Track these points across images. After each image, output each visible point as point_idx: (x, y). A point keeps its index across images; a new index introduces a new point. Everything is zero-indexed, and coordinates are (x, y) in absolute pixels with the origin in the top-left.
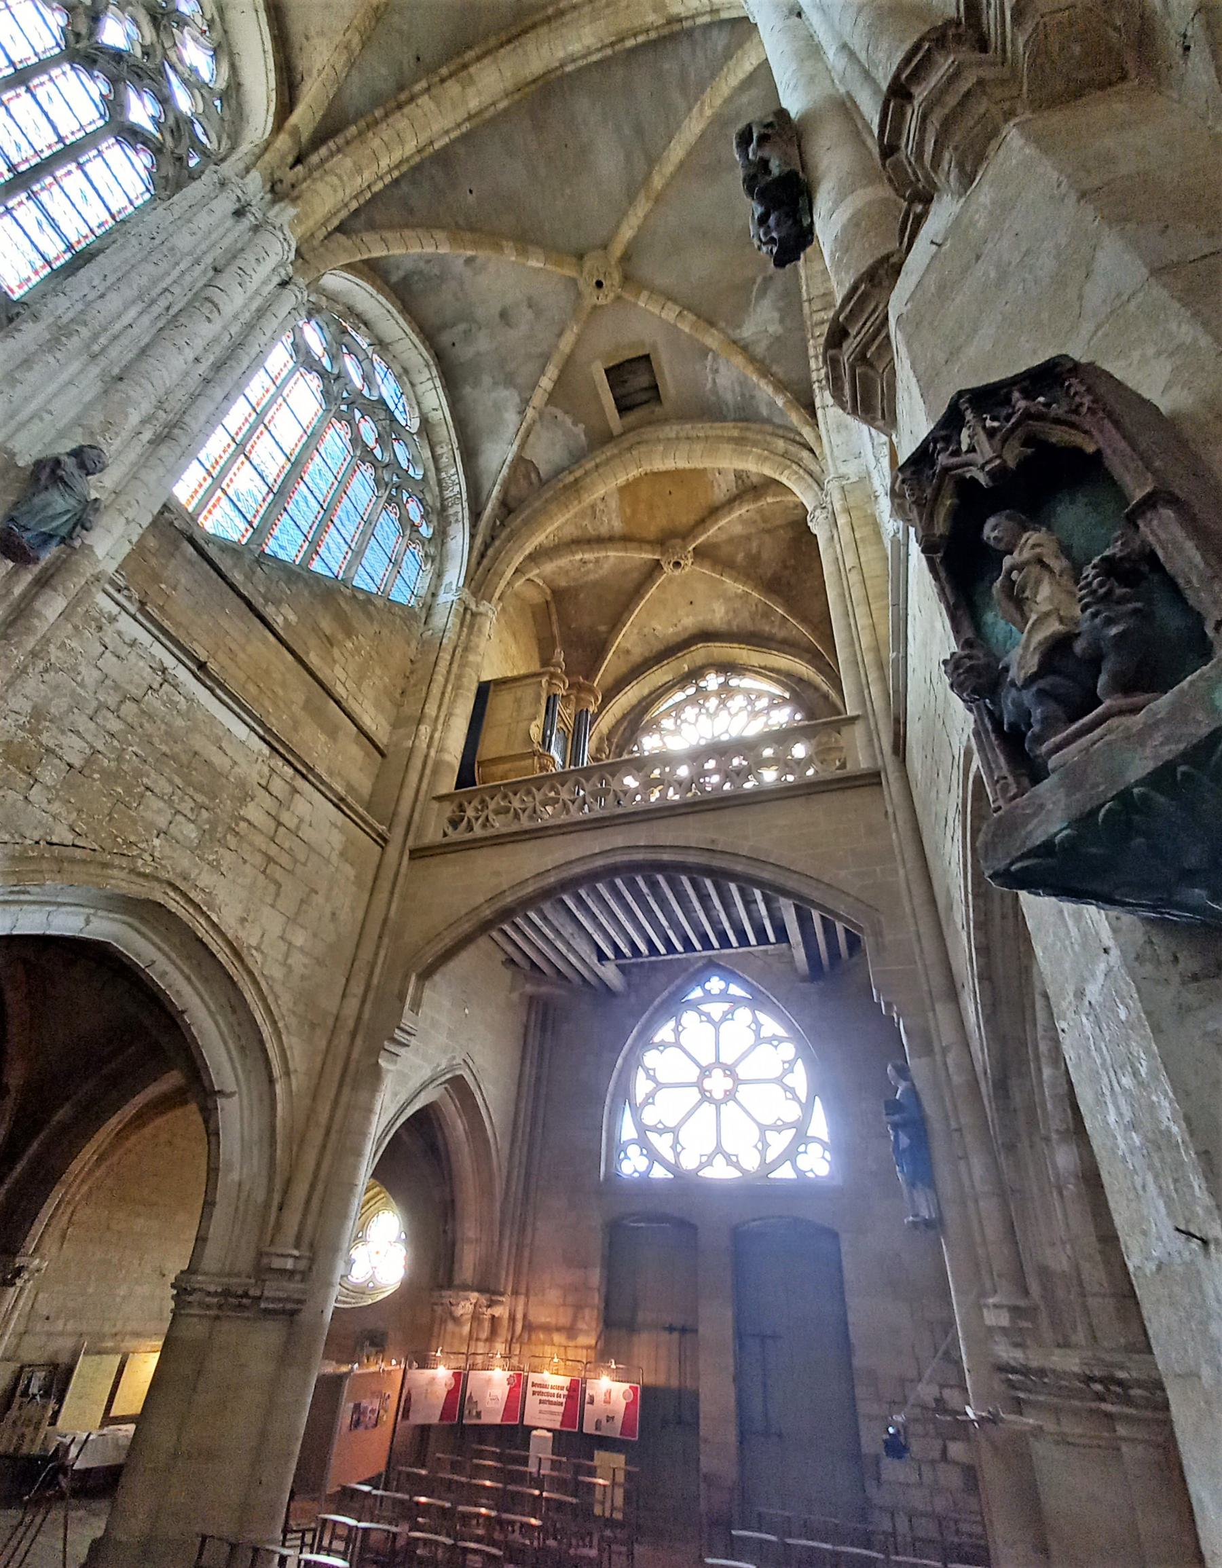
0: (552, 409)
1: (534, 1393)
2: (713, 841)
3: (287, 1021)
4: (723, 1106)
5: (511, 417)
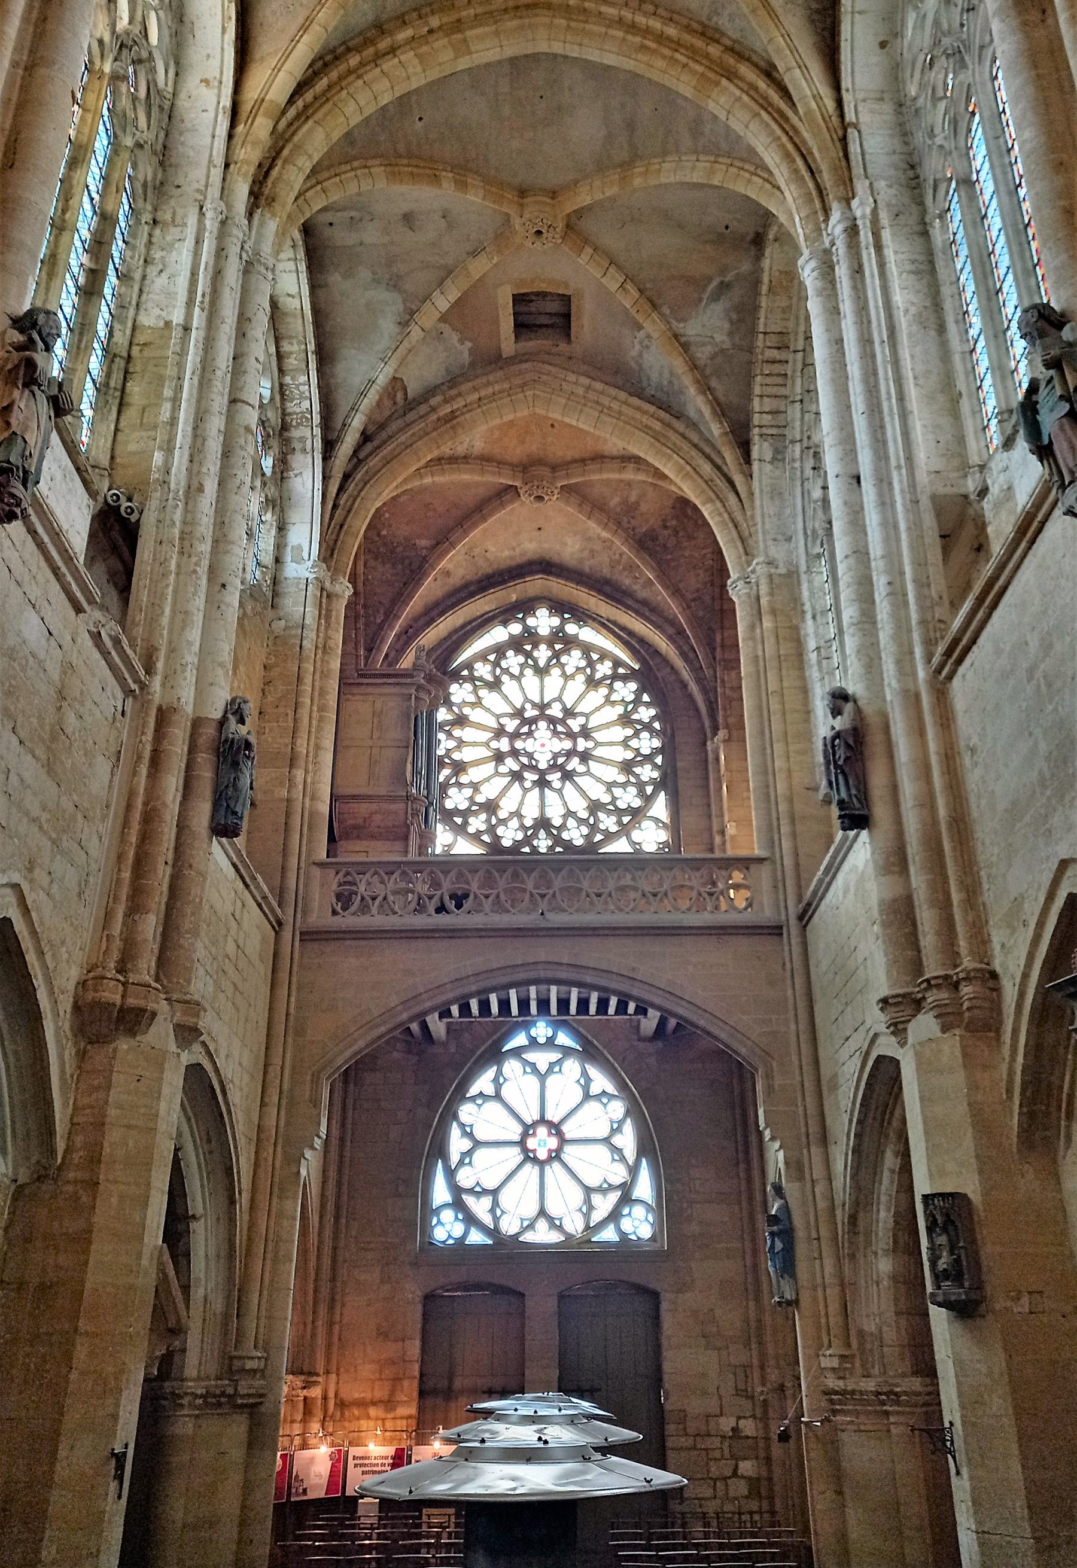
0: (446, 328)
1: (356, 1466)
2: (633, 969)
3: (242, 1141)
4: (547, 1168)
5: (388, 326)
